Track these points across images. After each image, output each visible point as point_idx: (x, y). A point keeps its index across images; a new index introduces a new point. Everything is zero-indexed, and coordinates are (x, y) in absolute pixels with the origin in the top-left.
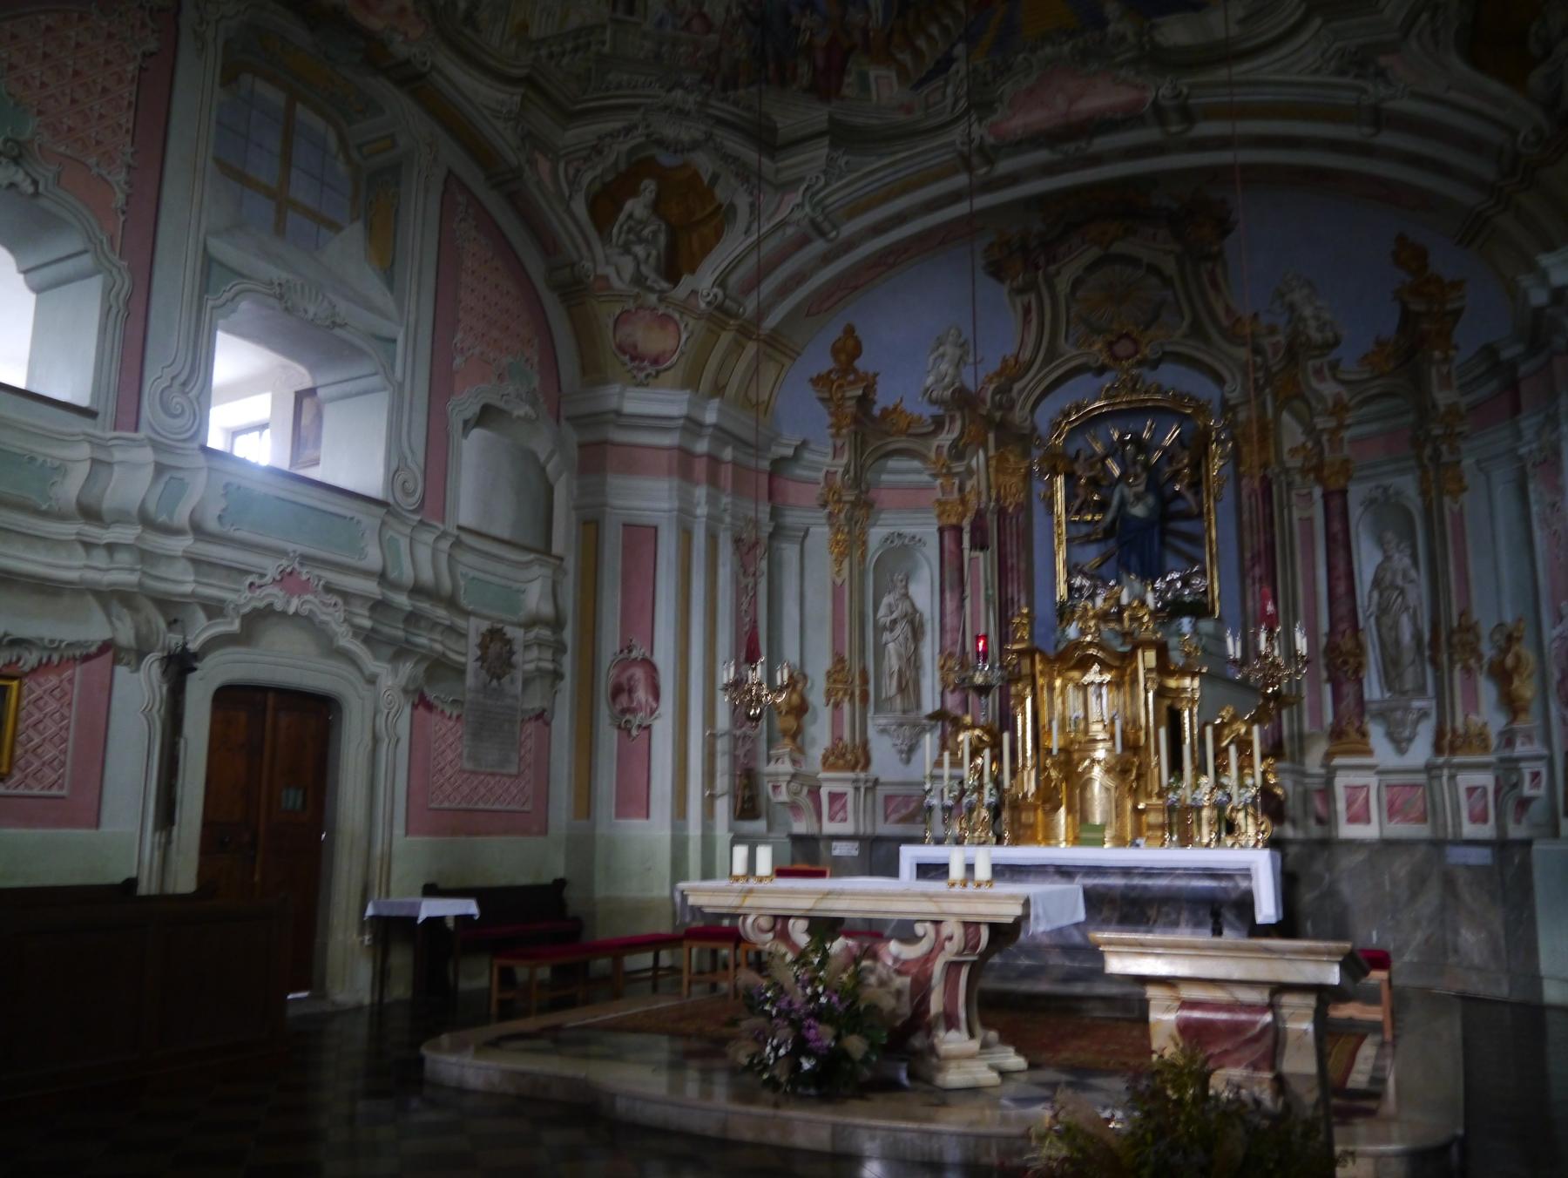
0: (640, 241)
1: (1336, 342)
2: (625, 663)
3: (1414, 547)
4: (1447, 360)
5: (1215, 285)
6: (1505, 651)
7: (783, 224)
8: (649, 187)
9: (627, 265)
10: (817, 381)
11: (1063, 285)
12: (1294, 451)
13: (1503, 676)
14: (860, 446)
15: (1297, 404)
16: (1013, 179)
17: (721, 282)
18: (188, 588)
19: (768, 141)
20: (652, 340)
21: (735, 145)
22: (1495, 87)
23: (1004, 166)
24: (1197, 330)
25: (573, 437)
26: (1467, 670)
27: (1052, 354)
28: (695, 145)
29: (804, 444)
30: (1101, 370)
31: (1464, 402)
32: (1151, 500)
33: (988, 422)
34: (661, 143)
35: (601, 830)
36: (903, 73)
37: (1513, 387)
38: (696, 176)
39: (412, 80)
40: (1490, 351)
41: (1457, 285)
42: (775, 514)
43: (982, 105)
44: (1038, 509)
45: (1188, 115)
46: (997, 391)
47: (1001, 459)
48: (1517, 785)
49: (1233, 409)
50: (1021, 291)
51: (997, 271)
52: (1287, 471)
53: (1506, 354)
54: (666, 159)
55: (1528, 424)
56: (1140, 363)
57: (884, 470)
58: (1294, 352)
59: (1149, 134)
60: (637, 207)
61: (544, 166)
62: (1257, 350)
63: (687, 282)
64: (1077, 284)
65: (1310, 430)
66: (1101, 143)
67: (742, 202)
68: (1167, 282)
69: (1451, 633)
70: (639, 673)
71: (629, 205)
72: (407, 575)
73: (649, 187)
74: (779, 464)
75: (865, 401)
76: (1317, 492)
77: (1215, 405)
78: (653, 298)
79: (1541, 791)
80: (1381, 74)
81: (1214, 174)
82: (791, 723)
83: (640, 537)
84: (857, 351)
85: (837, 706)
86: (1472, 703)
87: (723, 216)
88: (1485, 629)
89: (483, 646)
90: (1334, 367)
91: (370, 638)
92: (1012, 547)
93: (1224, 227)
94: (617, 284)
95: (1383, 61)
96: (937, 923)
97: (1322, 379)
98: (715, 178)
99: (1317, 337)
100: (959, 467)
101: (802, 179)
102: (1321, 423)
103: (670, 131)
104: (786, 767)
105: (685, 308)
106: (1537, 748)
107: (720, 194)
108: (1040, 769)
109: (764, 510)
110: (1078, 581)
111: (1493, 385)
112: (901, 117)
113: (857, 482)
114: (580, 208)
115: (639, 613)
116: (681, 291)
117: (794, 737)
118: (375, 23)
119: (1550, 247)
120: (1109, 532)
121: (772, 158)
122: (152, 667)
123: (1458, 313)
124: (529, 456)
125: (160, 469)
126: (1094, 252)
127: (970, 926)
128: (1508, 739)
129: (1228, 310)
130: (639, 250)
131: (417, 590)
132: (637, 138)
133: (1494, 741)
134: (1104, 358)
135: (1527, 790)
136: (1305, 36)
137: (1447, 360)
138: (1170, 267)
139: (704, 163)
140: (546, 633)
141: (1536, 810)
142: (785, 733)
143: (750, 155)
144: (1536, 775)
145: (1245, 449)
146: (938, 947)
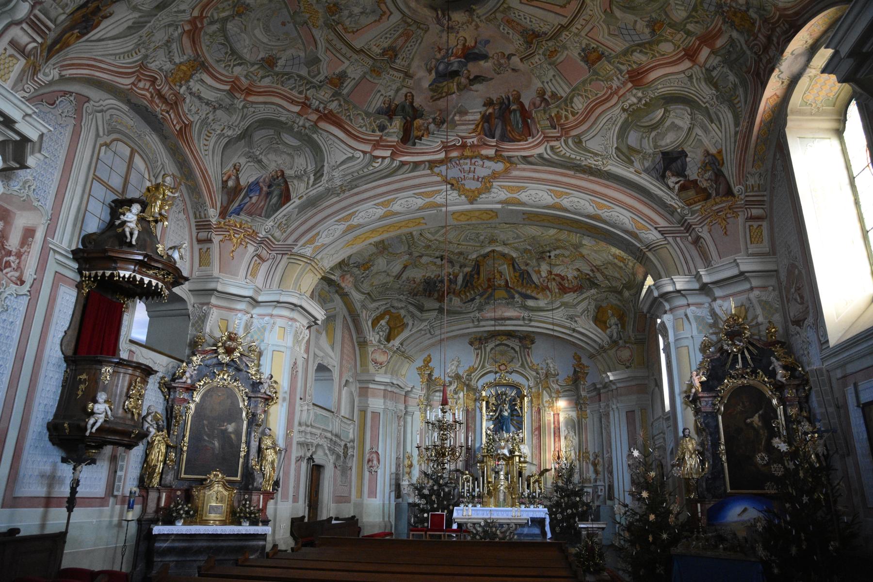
0: (382, 331)
1: (558, 375)
2: (371, 453)
3: (575, 430)
4: (584, 384)
5: (528, 355)
6: (595, 459)
7: (421, 330)
8: (387, 317)
9: (377, 337)
10: (419, 369)
11: (488, 349)
12: (546, 401)
13: (595, 465)
14: (428, 388)
15: (548, 389)
16: (484, 326)
17: (402, 344)
18: (309, 441)
19: (421, 309)
20: (382, 358)
21: (412, 309)
22: (600, 330)
23: (482, 323)
24: (522, 365)
25: (358, 385)
26: (587, 463)
27: (483, 367)
28: (402, 308)
29: (414, 387)
30: (496, 373)
31: (588, 396)
32: (509, 411)
33: (464, 384)
34: (393, 307)
35: (365, 502)
36: (462, 300)
37: (599, 394)
38: (400, 315)
39: (344, 295)
40: (594, 384)
41: (587, 367)
42: (406, 408)
43: (480, 309)
44: (478, 410)
45: (530, 320)
46: (467, 375)
47: (468, 395)
48: (597, 492)
49: (531, 388)
50: (476, 349)
51: (471, 344)
52: (544, 407)
53: (598, 386)
54: (393, 310)
55: (602, 404)
56: (507, 372)
57: (435, 396)
58: (547, 376)
59: (521, 322)
60: (383, 322)
61: (364, 312)
62: (538, 373)
63: (392, 342)
64: (492, 349)
65: (551, 396)
66: (508, 322)
67: (410, 323)
68: (516, 352)
69: (583, 453)
70: (375, 456)
71: (381, 322)
72: (334, 432)
73: (387, 317)
74: (407, 393)
75: (430, 375)
76: (552, 413)
77: (527, 387)
78: (382, 346)
79: (603, 494)
80: (576, 321)
81: (533, 332)
82: (407, 470)
83: (376, 415)
84: (430, 361)
85: (420, 465)
86: (588, 471)
87: (405, 325)
88: (591, 453)
89: (344, 449)
90: (557, 381)
91: (330, 449)
92: (470, 421)
93: (533, 342)
94: (374, 342)
95: (576, 319)
96: (508, 524)
97: (554, 383)
98: (405, 316)
99: (553, 372)
100: (456, 396)
101: (428, 319)
102: (553, 395)
103: (396, 304)
104: (407, 483)
105: (390, 349)
106: (602, 483)
107: (405, 321)
108: (488, 487)
109: (402, 407)
110: (489, 432)
111: (594, 393)
112: (459, 309)
113: (428, 399)
114: (370, 323)
115: (375, 438)
116: (390, 345)
117: (409, 474)
118: (343, 285)
119: (610, 371)
120: (497, 418)
121: (421, 313)
122: (305, 461)
123: (587, 373)
124: (351, 393)
125: (308, 410)
126: (498, 342)
127: (516, 525)
128: (596, 480)
129: (531, 362)
130: (381, 333)
131: (336, 436)
132: (388, 305)
133: (592, 481)
134: (497, 369)
135: (599, 494)
136: (560, 310)
137: (584, 384)
138: (517, 349)
139: (403, 312)
140: (352, 443)
141: (601, 497)
142: (407, 473)
143: (418, 313)
144: (602, 490)
145: (534, 400)
146: (509, 529)
